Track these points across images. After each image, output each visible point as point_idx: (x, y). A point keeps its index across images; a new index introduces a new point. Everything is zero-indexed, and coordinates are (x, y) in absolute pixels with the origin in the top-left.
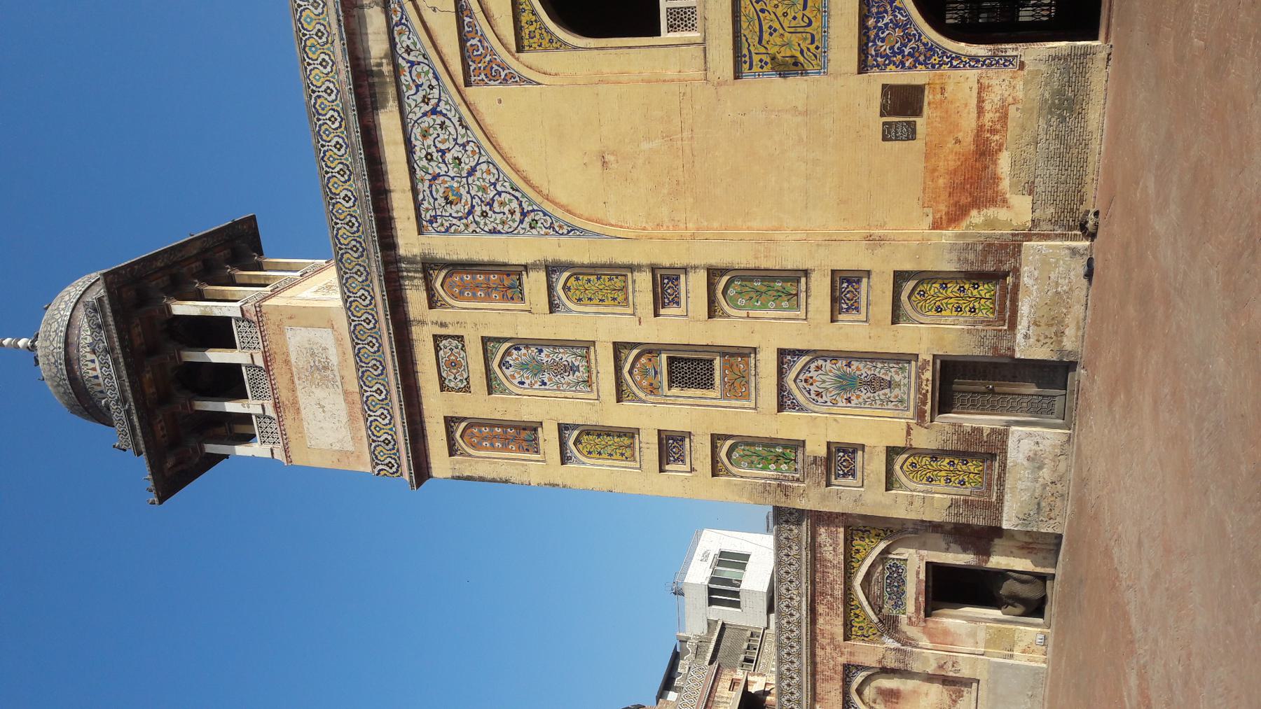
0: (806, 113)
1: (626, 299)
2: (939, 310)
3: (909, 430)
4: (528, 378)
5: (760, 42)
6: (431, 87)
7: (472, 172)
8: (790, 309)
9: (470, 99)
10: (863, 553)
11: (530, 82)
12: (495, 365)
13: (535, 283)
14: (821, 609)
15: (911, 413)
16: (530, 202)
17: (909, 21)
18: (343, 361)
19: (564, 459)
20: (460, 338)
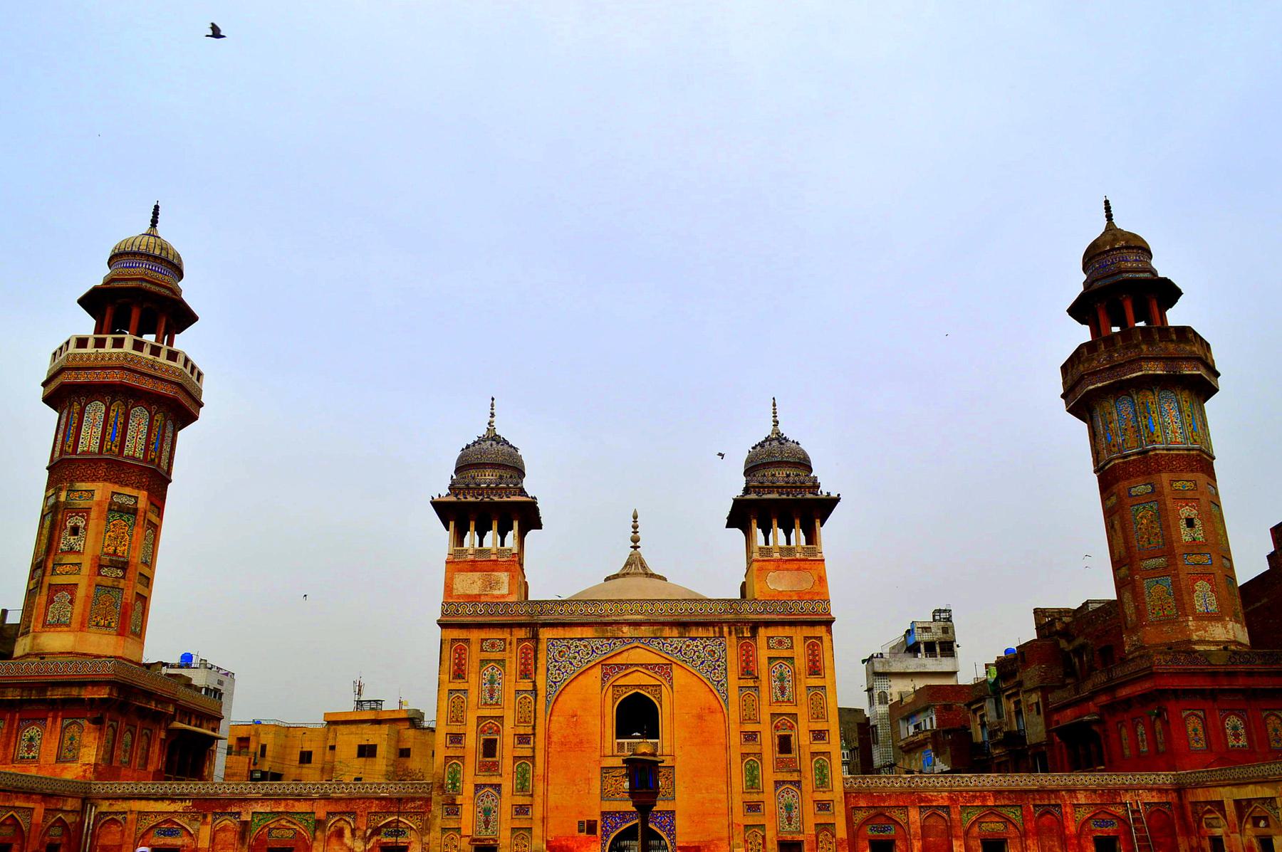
0: (589, 793)
1: (521, 722)
2: (517, 845)
3: (469, 836)
4: (487, 677)
5: (613, 776)
6: (602, 651)
7: (571, 663)
8: (517, 788)
9: (597, 666)
11: (602, 689)
12: (492, 664)
13: (526, 685)
14: (384, 803)
15: (474, 836)
16: (559, 686)
17: (617, 828)
18: (493, 596)
19: (451, 691)
20: (504, 650)
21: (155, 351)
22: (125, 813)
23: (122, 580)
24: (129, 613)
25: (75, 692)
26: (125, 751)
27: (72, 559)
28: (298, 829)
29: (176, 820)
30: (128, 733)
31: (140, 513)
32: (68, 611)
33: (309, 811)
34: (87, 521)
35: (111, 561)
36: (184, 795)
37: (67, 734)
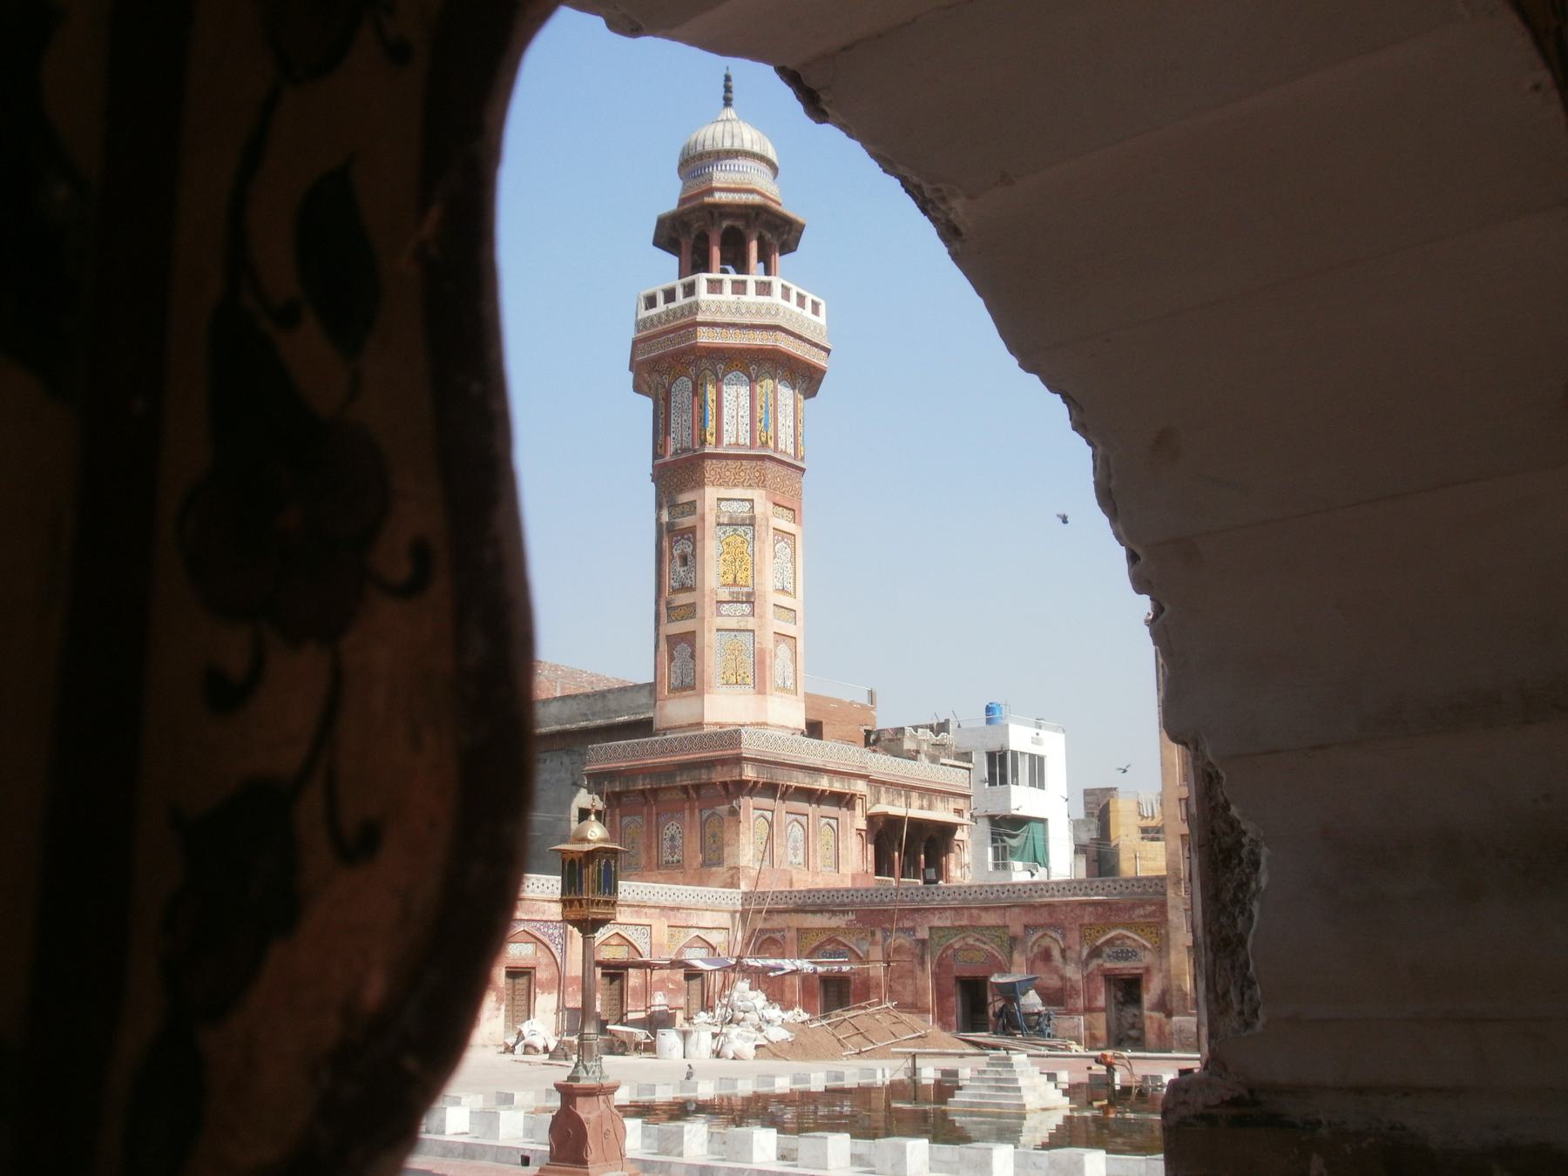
10: (1141, 933)
14: (1100, 909)
21: (739, 287)
22: (783, 930)
23: (750, 619)
24: (768, 661)
25: (704, 776)
26: (795, 849)
27: (682, 599)
28: (990, 950)
29: (840, 938)
30: (795, 823)
31: (758, 521)
32: (691, 669)
33: (1001, 923)
34: (694, 544)
35: (732, 594)
36: (845, 905)
37: (707, 830)
